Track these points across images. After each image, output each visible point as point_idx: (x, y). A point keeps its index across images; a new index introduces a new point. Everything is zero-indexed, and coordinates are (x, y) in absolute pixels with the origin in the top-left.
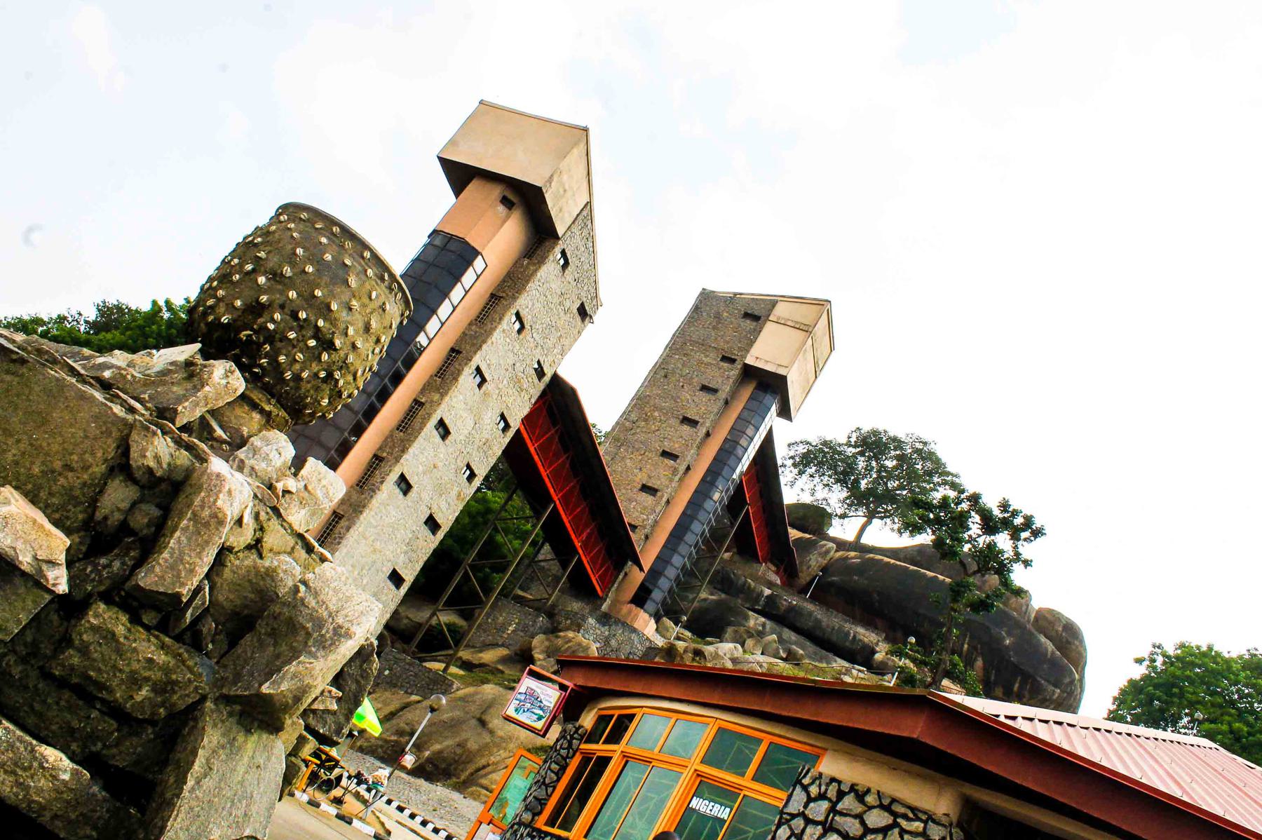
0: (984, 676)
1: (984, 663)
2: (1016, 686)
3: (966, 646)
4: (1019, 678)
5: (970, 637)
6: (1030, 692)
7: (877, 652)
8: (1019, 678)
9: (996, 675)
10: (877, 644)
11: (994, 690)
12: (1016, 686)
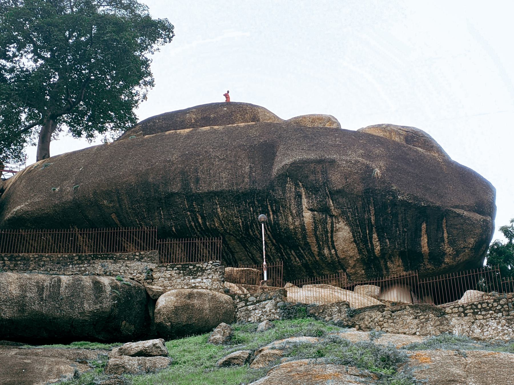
0: (360, 251)
1: (353, 231)
2: (424, 240)
3: (307, 215)
4: (424, 226)
5: (308, 197)
6: (452, 243)
7: (159, 294)
8: (424, 226)
9: (381, 239)
10: (150, 278)
11: (387, 268)
12: (424, 240)
